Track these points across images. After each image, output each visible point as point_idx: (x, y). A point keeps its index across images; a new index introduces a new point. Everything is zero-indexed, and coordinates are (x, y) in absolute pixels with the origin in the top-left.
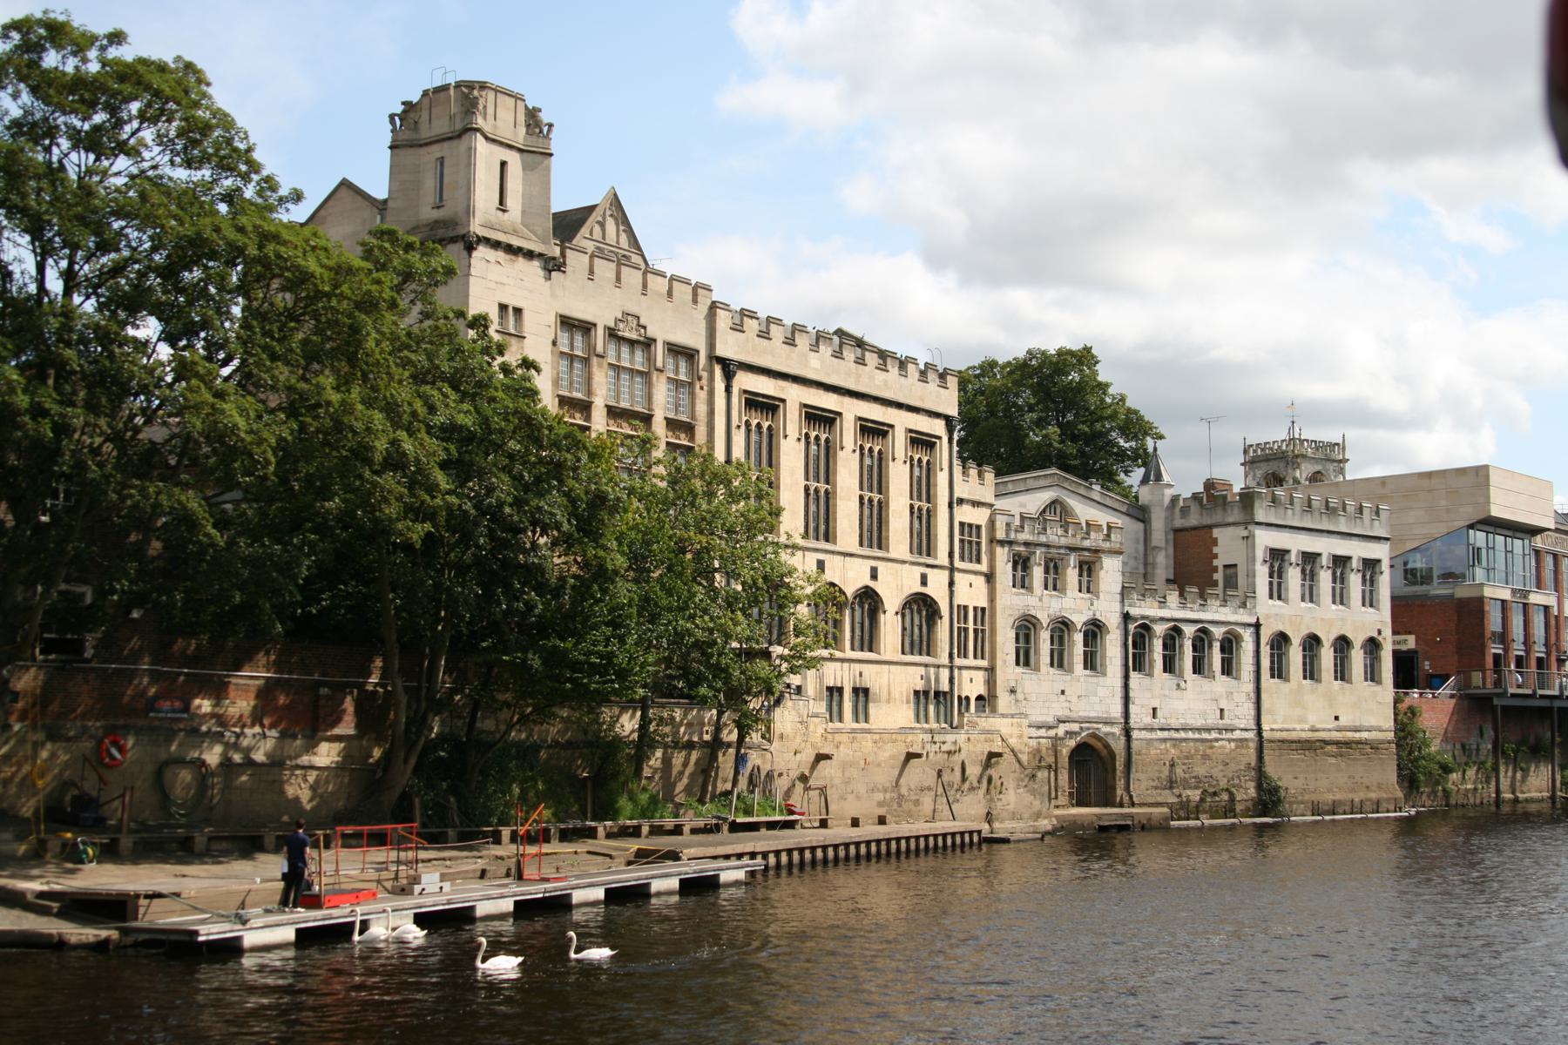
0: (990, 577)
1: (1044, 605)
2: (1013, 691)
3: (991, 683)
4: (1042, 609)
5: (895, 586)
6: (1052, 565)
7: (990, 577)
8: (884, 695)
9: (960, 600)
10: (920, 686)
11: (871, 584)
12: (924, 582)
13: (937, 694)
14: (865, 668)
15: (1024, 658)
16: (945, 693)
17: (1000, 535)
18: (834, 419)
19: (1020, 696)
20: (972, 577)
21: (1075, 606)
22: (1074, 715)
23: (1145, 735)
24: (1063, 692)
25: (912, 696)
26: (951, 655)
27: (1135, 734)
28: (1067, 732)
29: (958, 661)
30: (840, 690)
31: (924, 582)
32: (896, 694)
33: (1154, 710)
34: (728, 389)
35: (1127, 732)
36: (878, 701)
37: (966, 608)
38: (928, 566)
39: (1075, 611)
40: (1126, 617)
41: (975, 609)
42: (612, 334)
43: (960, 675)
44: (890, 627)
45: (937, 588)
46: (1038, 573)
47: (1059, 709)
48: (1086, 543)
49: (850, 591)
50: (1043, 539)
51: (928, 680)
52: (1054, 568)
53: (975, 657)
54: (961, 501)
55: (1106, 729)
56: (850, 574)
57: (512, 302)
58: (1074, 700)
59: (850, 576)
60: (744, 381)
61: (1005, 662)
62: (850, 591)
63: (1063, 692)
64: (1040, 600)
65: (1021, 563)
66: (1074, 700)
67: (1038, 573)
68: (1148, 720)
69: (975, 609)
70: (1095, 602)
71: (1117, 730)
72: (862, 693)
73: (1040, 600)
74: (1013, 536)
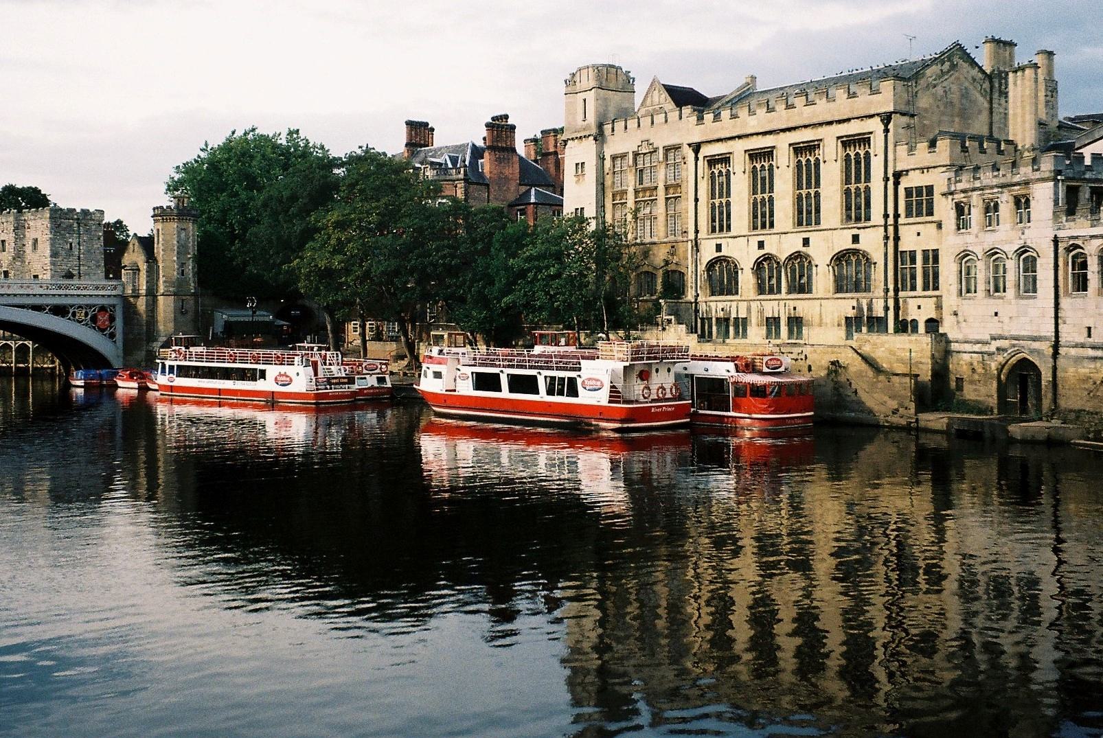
0: (939, 226)
1: (977, 240)
2: (956, 314)
3: (939, 307)
4: (976, 244)
5: (823, 247)
6: (992, 204)
7: (939, 226)
8: (816, 320)
9: (904, 246)
10: (851, 313)
11: (804, 249)
12: (856, 239)
13: (870, 318)
14: (799, 304)
15: (967, 286)
16: (878, 318)
17: (945, 190)
18: (772, 151)
19: (961, 318)
20: (920, 228)
21: (1006, 236)
22: (1006, 334)
23: (1073, 352)
24: (996, 314)
25: (843, 322)
26: (887, 290)
27: (1062, 351)
28: (998, 349)
29: (901, 294)
30: (779, 318)
31: (856, 239)
32: (827, 319)
33: (1089, 329)
34: (697, 159)
35: (1056, 346)
36: (810, 325)
37: (913, 255)
38: (859, 228)
39: (1007, 242)
40: (1056, 241)
41: (925, 252)
42: (636, 155)
43: (905, 302)
44: (823, 279)
45: (872, 242)
46: (976, 215)
47: (994, 328)
48: (1017, 179)
49: (783, 257)
50: (977, 184)
51: (860, 309)
52: (991, 208)
53: (926, 288)
54: (898, 175)
55: (1036, 345)
56: (785, 246)
57: (580, 162)
58: (1006, 320)
59: (783, 244)
60: (707, 151)
61: (948, 291)
62: (783, 257)
63: (996, 314)
64: (977, 237)
65: (960, 209)
66: (1006, 320)
67: (976, 215)
68: (1081, 338)
69: (925, 252)
70: (1026, 231)
71: (1046, 348)
72: (796, 323)
73: (977, 237)
74: (953, 188)
